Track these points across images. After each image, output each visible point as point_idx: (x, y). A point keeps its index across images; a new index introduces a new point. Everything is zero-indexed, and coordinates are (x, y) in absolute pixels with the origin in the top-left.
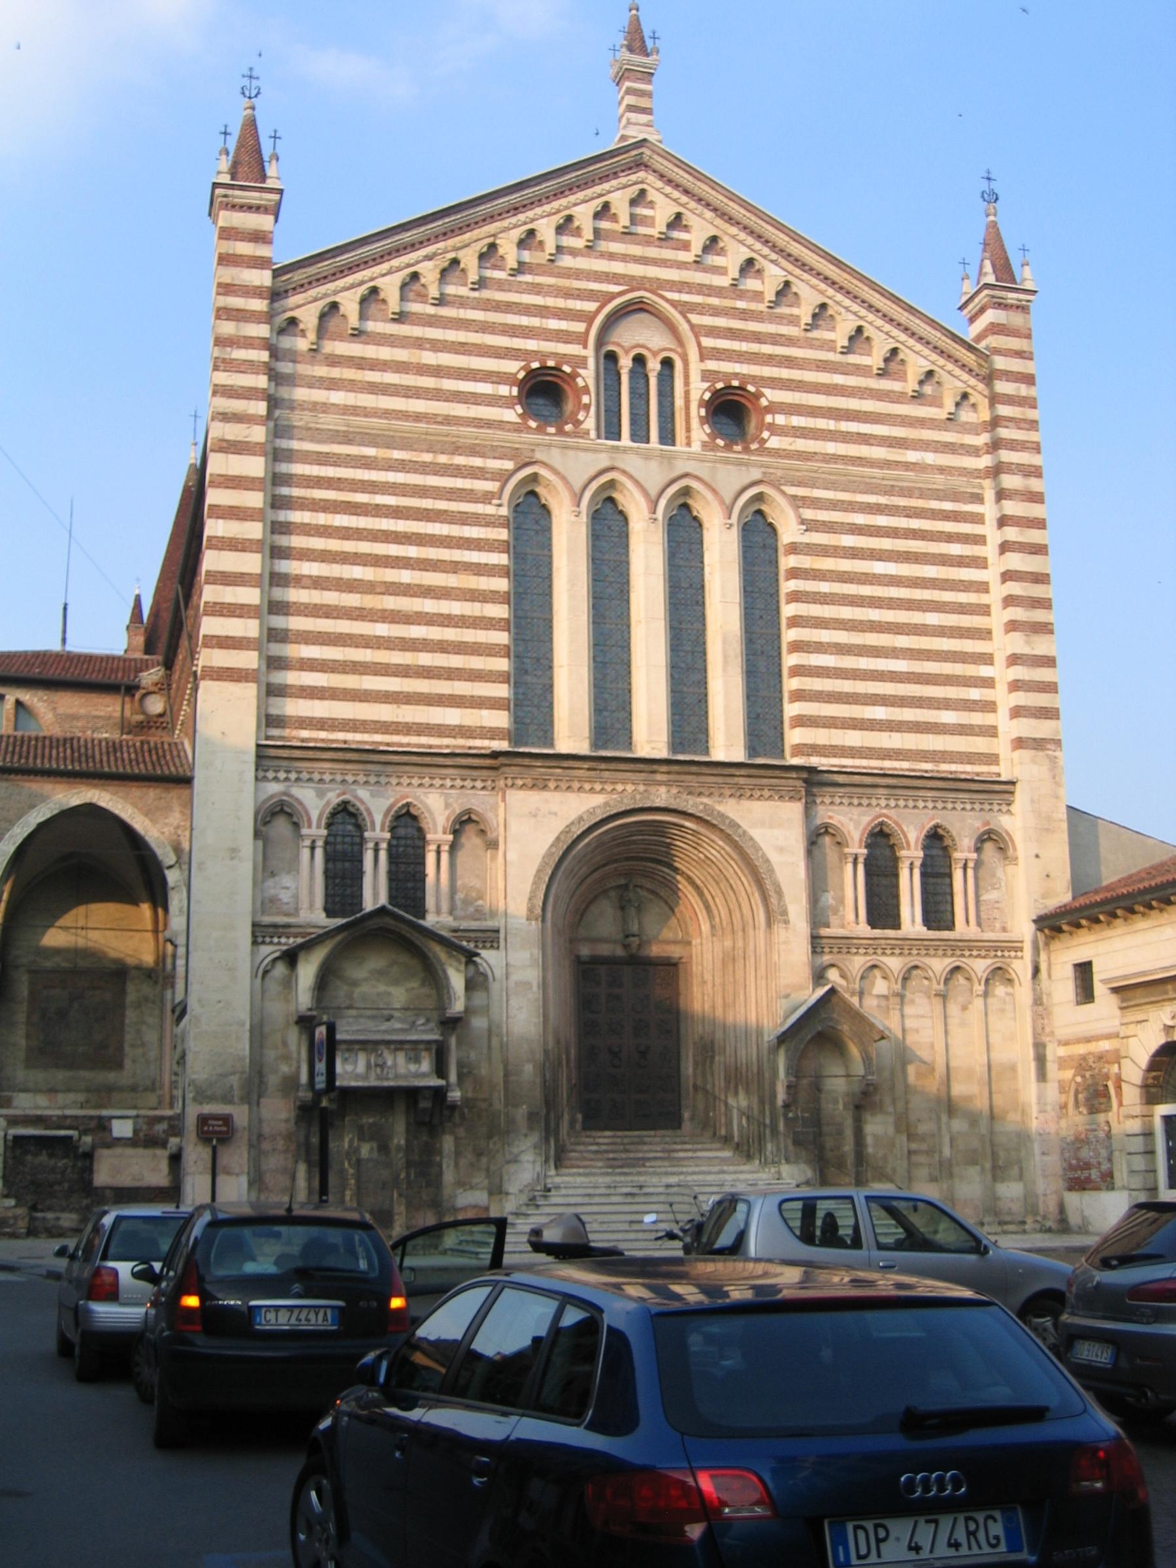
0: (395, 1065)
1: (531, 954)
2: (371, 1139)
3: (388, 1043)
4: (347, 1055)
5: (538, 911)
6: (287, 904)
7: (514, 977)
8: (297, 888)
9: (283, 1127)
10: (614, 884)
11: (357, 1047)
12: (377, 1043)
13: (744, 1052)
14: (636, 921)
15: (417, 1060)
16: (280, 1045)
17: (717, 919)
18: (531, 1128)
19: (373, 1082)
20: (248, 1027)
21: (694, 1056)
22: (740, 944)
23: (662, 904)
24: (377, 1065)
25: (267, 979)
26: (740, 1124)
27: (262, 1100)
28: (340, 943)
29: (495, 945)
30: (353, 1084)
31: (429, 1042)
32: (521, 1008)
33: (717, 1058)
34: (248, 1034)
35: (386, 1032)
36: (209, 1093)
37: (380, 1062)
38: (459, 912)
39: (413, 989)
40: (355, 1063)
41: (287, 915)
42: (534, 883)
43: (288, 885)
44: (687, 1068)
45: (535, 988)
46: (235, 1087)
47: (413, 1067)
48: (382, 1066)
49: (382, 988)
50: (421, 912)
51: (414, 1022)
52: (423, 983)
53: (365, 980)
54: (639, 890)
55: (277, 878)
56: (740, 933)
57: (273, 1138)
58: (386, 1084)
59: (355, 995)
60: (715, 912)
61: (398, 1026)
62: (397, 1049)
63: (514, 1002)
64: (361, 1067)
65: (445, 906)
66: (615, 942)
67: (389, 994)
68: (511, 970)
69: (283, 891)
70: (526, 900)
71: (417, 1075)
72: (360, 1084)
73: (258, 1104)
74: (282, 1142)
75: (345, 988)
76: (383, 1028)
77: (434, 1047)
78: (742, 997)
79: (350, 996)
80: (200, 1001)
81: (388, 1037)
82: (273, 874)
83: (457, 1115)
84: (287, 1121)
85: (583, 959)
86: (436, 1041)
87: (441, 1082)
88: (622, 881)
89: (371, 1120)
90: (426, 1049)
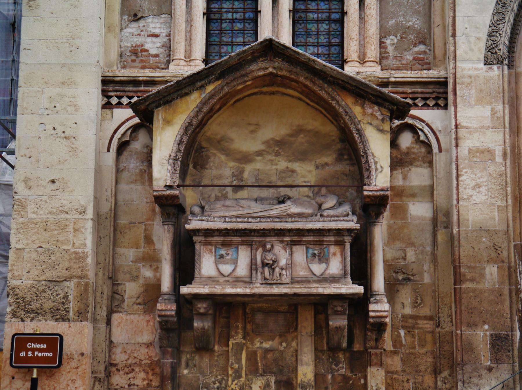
0: (290, 266)
1: (493, 112)
2: (265, 373)
3: (280, 233)
4: (223, 252)
5: (503, 50)
6: (157, 56)
7: (466, 145)
8: (169, 35)
9: (143, 353)
11: (239, 239)
12: (264, 233)
15: (323, 259)
16: (142, 241)
18: (497, 360)
19: (259, 289)
20: (90, 213)
24: (264, 265)
25: (125, 153)
27: (115, 317)
28: (211, 96)
29: (441, 103)
30: (229, 290)
31: (339, 232)
32: (478, 186)
34: (90, 224)
35: (280, 218)
36: (34, 306)
37: (269, 257)
38: (391, 62)
39: (326, 164)
40: (235, 262)
41: (155, 67)
42: (497, 12)
43: (157, 31)
45: (499, 159)
46: (71, 298)
47: (317, 268)
48: (271, 266)
49: (283, 164)
50: (342, 62)
51: (320, 206)
52: (339, 159)
53: (259, 153)
55: (142, 23)
57: (130, 369)
58: (276, 290)
59: (246, 175)
61: (295, 209)
62: (294, 243)
63: (466, 179)
64: (242, 270)
65: (373, 52)
67: (293, 171)
68: (462, 133)
69: (149, 39)
70: (484, 36)
71: (323, 280)
72: (239, 290)
73: (109, 322)
74: (142, 375)
75: (232, 164)
76: (274, 213)
77: (348, 240)
79: (239, 175)
80: (26, 181)
81: (279, 226)
82: (136, 18)
83: (387, 336)
84: (149, 345)
86: (350, 231)
87: (360, 289)
89: (267, 345)
90: (340, 244)
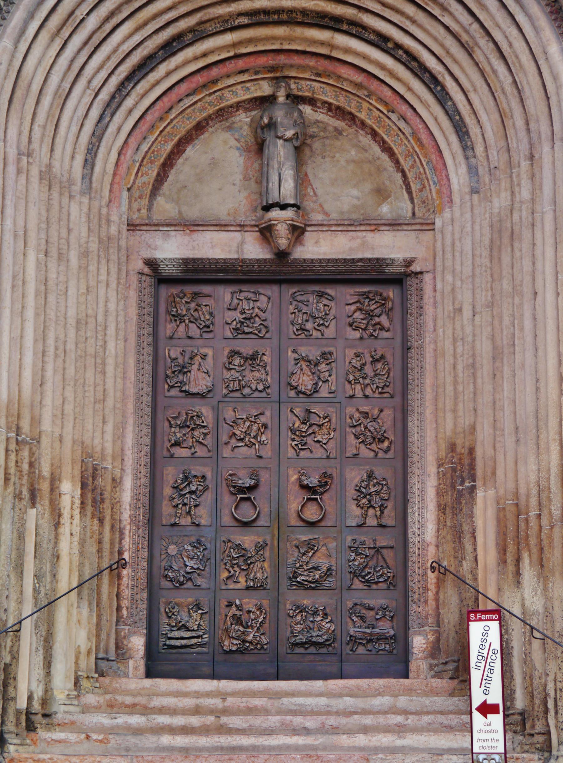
10: (243, 95)
13: (533, 467)
14: (288, 174)
17: (479, 149)
21: (439, 494)
22: (525, 194)
23: (366, 140)
26: (527, 660)
33: (480, 494)
44: (422, 525)
54: (307, 109)
56: (525, 164)
60: (474, 130)
66: (242, 227)
78: (528, 324)
85: (168, 270)
88: (266, 89)
